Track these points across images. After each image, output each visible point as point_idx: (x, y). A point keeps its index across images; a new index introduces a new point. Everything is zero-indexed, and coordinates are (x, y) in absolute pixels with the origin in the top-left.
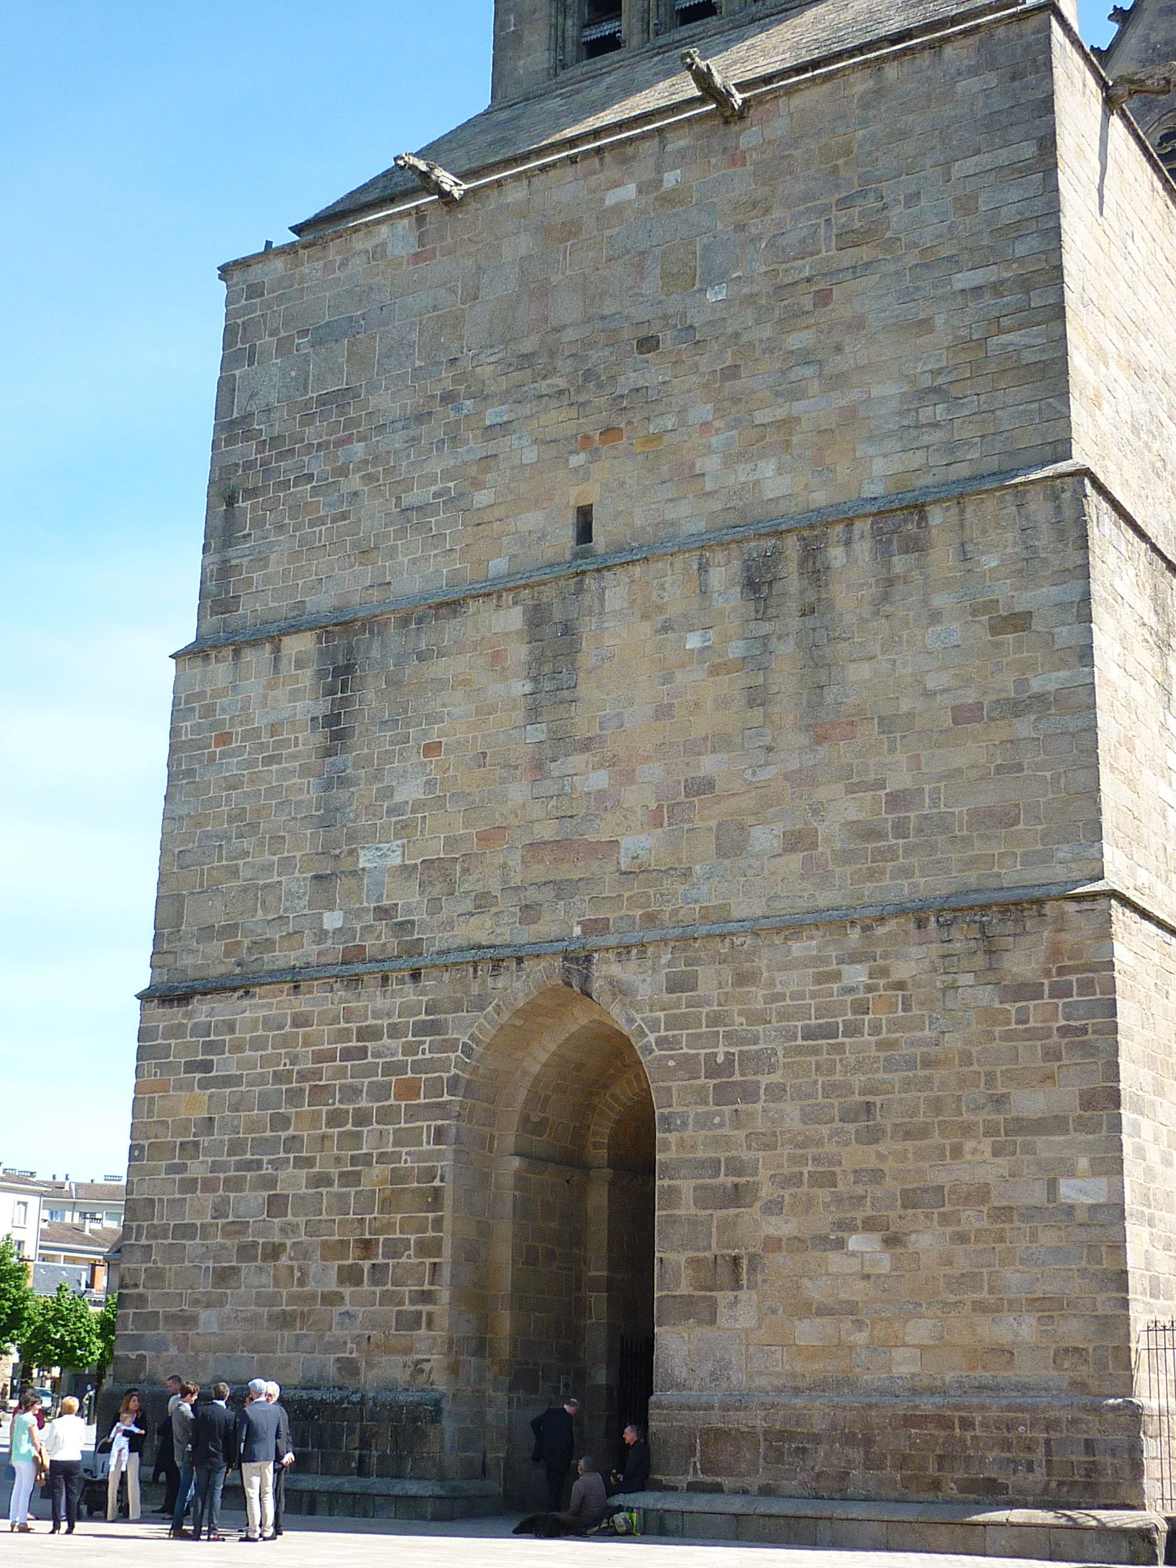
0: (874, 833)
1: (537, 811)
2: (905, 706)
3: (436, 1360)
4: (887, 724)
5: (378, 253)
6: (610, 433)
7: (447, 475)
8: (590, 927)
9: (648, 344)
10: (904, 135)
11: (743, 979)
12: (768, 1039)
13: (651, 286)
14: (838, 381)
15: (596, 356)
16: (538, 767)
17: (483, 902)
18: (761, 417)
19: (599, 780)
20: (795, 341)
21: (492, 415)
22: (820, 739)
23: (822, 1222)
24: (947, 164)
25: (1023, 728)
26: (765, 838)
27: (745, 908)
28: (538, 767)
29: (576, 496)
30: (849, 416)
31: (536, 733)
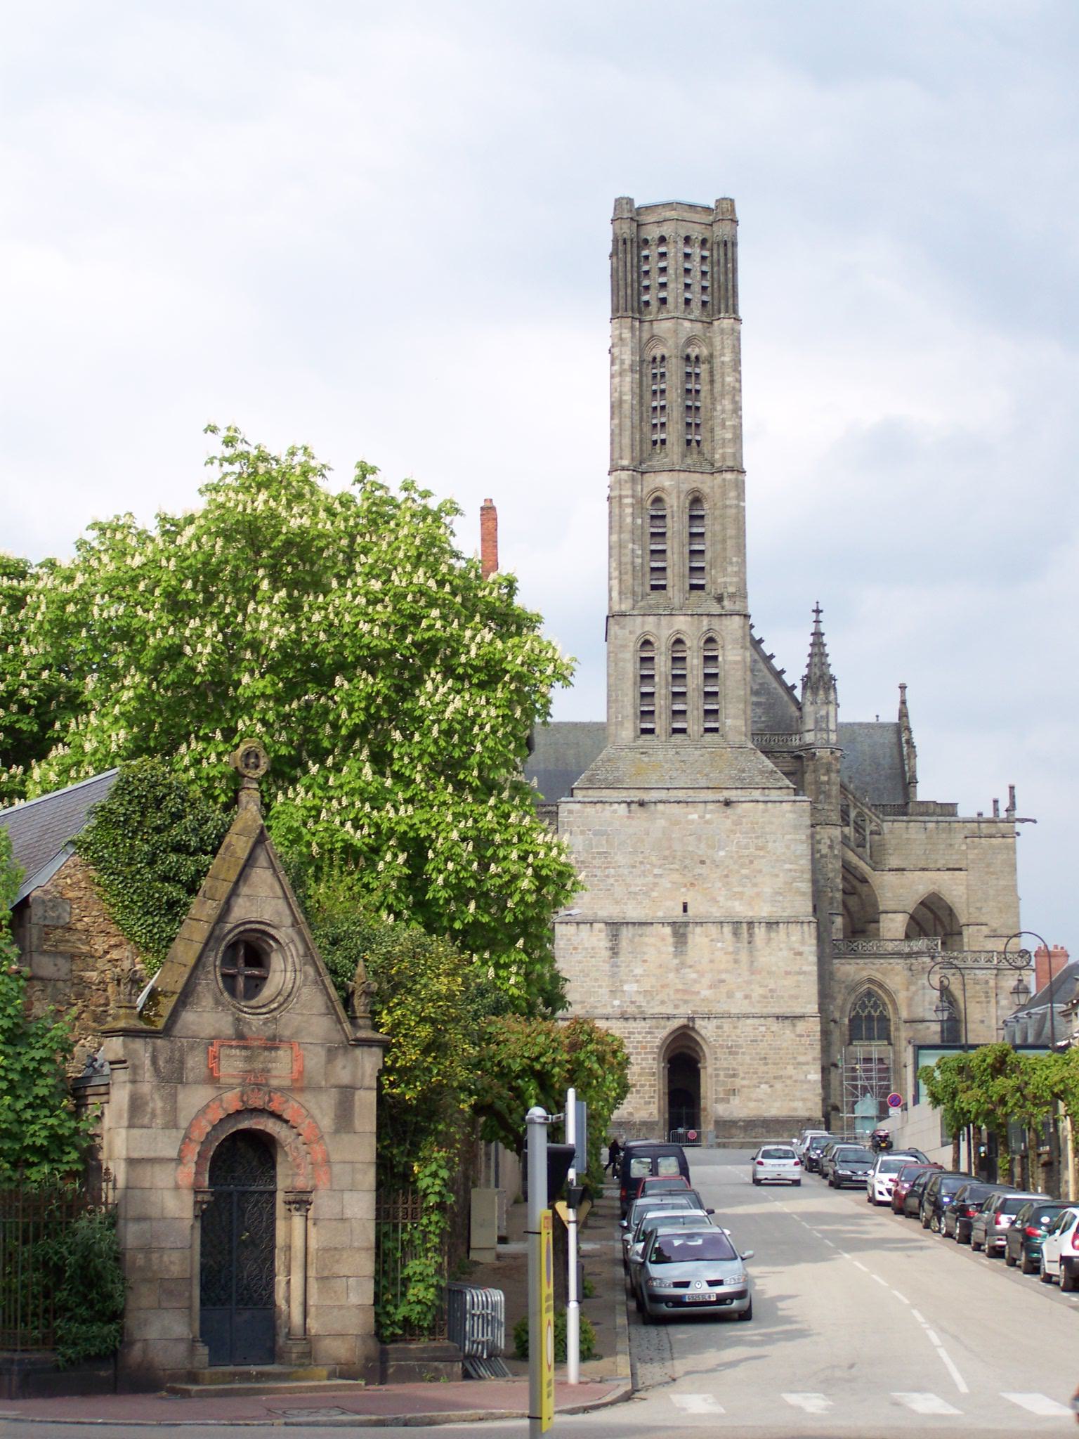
0: (765, 997)
1: (677, 981)
2: (774, 969)
3: (656, 1112)
4: (769, 973)
5: (615, 812)
6: (692, 884)
7: (643, 885)
8: (694, 1012)
9: (703, 862)
10: (772, 823)
11: (735, 1028)
12: (741, 1041)
13: (703, 846)
14: (755, 885)
15: (688, 862)
16: (677, 970)
17: (663, 1002)
18: (736, 890)
19: (694, 976)
20: (744, 872)
21: (656, 871)
22: (752, 974)
23: (755, 1082)
24: (783, 836)
25: (801, 978)
26: (739, 995)
27: (734, 1011)
28: (677, 970)
29: (682, 900)
30: (758, 894)
31: (676, 961)
